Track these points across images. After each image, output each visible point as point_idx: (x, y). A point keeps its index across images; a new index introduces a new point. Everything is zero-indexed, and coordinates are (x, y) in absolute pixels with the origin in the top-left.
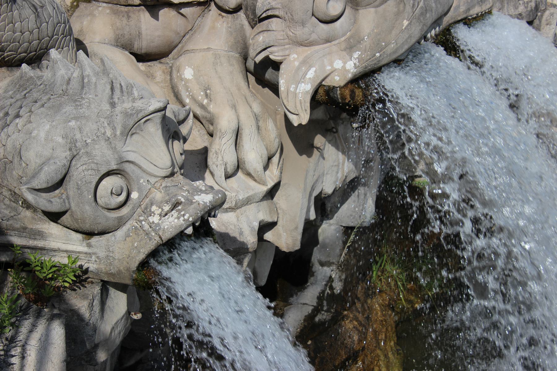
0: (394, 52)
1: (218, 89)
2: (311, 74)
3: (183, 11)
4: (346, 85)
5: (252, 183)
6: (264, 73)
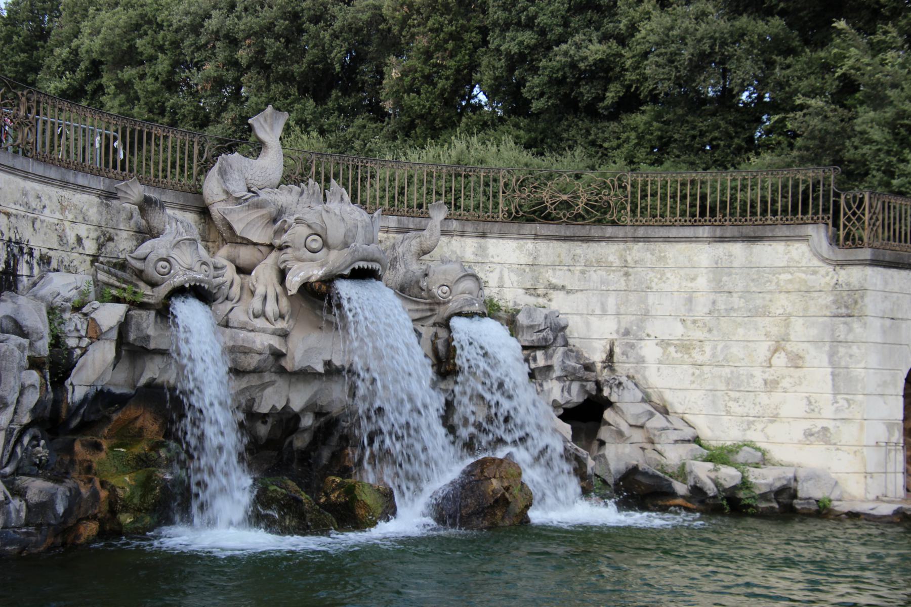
0: (339, 267)
1: (261, 278)
2: (302, 274)
3: (261, 248)
4: (317, 281)
5: (268, 324)
6: (282, 275)
